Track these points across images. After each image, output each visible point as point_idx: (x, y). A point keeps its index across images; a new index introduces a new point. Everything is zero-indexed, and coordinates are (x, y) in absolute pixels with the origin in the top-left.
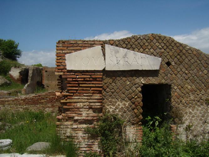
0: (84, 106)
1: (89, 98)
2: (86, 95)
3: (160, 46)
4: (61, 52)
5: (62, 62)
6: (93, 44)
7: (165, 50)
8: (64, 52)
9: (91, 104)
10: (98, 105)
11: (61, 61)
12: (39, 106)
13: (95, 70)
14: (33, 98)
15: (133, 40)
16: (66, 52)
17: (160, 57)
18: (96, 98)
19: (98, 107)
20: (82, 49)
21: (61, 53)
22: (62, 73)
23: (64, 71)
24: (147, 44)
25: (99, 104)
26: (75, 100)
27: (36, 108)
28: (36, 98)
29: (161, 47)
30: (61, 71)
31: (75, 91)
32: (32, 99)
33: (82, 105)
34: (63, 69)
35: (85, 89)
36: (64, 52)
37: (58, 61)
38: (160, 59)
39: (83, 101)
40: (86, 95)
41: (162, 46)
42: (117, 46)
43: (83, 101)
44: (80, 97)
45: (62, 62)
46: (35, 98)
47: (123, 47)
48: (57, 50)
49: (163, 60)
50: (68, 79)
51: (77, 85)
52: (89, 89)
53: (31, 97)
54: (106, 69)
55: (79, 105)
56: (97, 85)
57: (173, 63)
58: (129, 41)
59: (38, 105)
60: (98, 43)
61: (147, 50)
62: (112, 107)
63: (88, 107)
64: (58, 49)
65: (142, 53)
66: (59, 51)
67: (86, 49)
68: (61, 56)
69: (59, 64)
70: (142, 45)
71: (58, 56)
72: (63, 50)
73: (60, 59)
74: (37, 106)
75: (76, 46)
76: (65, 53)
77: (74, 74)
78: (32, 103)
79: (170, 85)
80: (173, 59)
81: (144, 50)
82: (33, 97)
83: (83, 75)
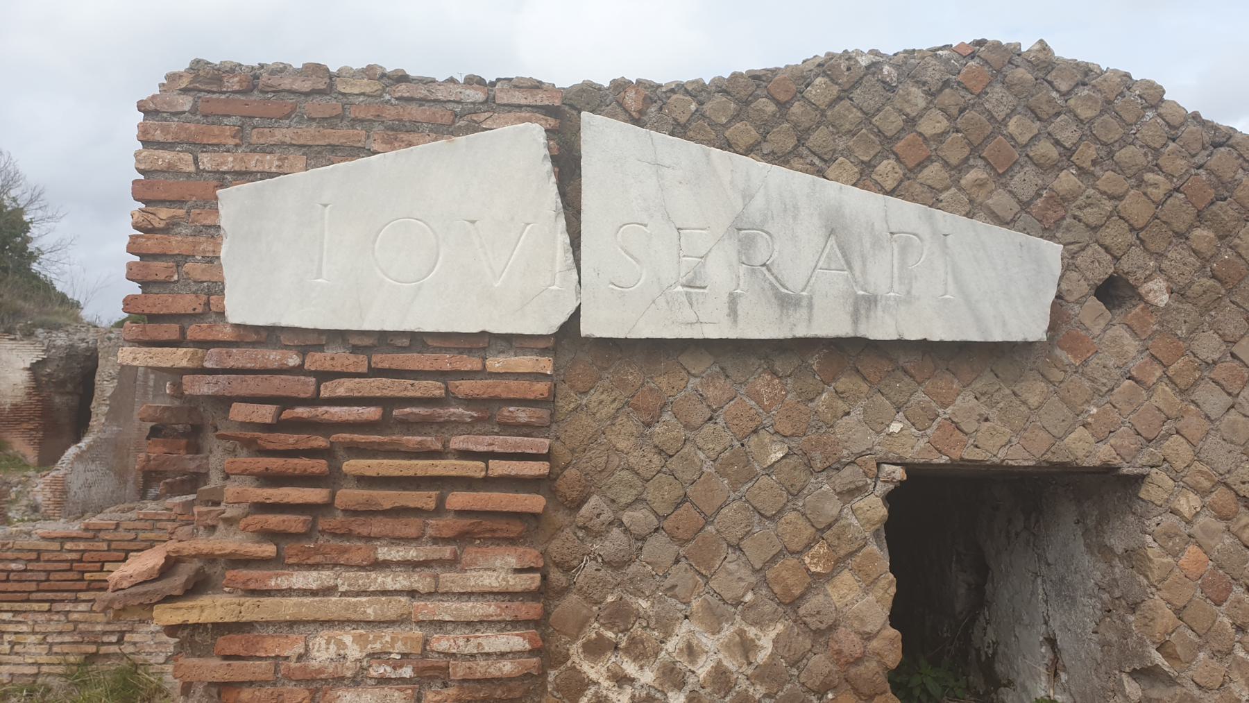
0: (372, 656)
1: (419, 581)
2: (396, 554)
3: (1045, 148)
4: (185, 162)
5: (186, 257)
6: (476, 108)
7: (1082, 172)
8: (206, 161)
9: (442, 643)
10: (502, 655)
11: (176, 243)
12: (82, 607)
13: (483, 334)
14: (39, 552)
15: (819, 89)
16: (229, 162)
17: (1048, 233)
18: (491, 581)
19: (507, 667)
20: (375, 147)
21: (179, 173)
22: (179, 357)
23: (201, 336)
24: (933, 124)
25: (516, 641)
26: (288, 608)
27: (60, 627)
28: (68, 546)
29: (1054, 153)
30: (170, 331)
31: (294, 523)
32: (33, 556)
33: (354, 652)
34: (194, 317)
35: (387, 505)
36: (206, 161)
37: (152, 244)
38: (1052, 251)
39: (370, 609)
40: (396, 554)
41: (1057, 143)
42: (680, 130)
43: (370, 609)
44: (345, 579)
45: (186, 257)
46: (55, 546)
47: (728, 146)
48: (147, 143)
49: (1069, 266)
50: (240, 412)
51: (318, 466)
52: (424, 499)
53: (34, 542)
54: (589, 328)
55: (322, 651)
56: (499, 468)
57: (1158, 292)
58: (782, 97)
59: (77, 601)
60: (518, 98)
61: (933, 172)
62: (630, 668)
63: (407, 672)
64: (158, 136)
65: (891, 193)
66: (167, 156)
67: (410, 144)
68: (180, 202)
69: (159, 269)
70: (890, 129)
71: (149, 196)
72: (204, 147)
73: (169, 228)
74: (68, 607)
75: (329, 121)
76: (223, 179)
77: (294, 360)
78: (33, 586)
79: (1138, 480)
80: (1160, 256)
81: (914, 172)
82: (43, 545)
83: (374, 372)
